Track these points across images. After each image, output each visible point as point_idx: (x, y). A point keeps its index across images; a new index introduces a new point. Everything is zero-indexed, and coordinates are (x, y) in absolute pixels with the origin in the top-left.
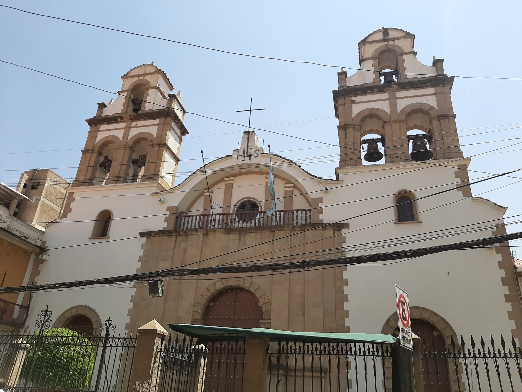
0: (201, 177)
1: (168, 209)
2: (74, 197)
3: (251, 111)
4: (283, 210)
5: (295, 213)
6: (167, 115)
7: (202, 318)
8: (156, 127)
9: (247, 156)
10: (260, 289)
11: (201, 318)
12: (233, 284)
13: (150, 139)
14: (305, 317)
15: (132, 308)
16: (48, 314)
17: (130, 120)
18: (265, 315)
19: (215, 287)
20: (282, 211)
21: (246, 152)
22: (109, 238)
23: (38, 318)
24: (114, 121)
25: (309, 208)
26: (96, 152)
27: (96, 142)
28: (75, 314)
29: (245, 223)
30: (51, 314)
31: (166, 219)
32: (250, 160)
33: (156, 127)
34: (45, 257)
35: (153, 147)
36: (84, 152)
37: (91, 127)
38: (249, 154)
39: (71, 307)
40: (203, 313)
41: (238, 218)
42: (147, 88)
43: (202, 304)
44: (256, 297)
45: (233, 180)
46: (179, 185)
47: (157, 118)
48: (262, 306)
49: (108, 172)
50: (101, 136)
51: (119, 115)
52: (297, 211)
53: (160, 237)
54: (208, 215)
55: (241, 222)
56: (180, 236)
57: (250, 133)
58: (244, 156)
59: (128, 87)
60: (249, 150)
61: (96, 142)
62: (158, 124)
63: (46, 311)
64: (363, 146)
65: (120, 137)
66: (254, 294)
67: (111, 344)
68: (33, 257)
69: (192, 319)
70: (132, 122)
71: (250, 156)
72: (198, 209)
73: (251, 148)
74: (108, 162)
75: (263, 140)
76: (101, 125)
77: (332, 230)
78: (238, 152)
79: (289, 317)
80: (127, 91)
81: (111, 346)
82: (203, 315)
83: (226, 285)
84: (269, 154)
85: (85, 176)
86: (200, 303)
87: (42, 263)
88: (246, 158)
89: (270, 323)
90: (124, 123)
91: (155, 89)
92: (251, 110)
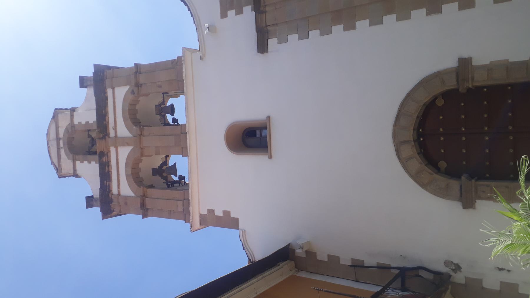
1: (224, 15)
2: (205, 212)
8: (117, 90)
13: (131, 97)
17: (105, 139)
22: (269, 118)
24: (107, 167)
31: (239, 12)
37: (114, 210)
42: (72, 127)
47: (105, 93)
53: (267, 9)
59: (70, 161)
68: (303, 275)
70: (109, 137)
76: (111, 192)
80: (74, 161)
87: (316, 253)
90: (110, 152)
91: (75, 113)
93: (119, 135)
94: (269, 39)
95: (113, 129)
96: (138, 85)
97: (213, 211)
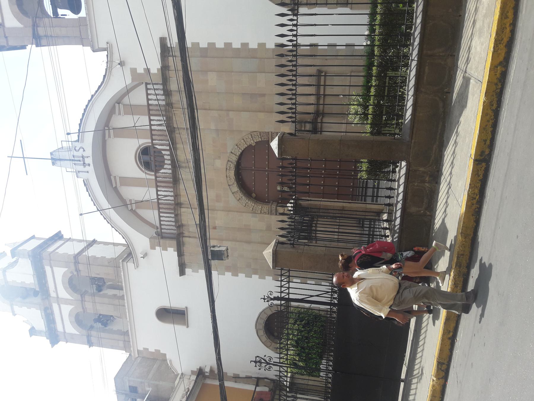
0: (112, 213)
1: (153, 247)
2: (142, 349)
3: (24, 157)
4: (148, 117)
5: (150, 102)
6: (39, 257)
7: (268, 204)
8: (55, 269)
9: (84, 161)
10: (238, 143)
11: (267, 205)
12: (233, 174)
13: (70, 275)
14: (265, 94)
15: (257, 276)
16: (259, 360)
18: (264, 138)
19: (237, 192)
20: (149, 118)
21: (79, 162)
23: (263, 370)
25: (144, 85)
26: (90, 333)
27: (78, 333)
28: (264, 331)
29: (166, 162)
30: (258, 357)
31: (165, 249)
32: (88, 157)
33: (55, 269)
34: (207, 370)
35: (80, 271)
36: (90, 344)
38: (81, 159)
39: (257, 336)
40: (263, 203)
41: (160, 170)
43: (253, 205)
44: (246, 148)
45: (115, 177)
46: (124, 238)
47: (43, 268)
48: (255, 141)
49: (113, 317)
50: (71, 329)
51: (43, 312)
52: (148, 100)
53: (185, 253)
54: (159, 204)
55: (165, 166)
56: (183, 233)
57: (54, 157)
58: (84, 164)
60: (76, 159)
61: (78, 333)
62: (51, 267)
63: (256, 362)
64: (62, 15)
65: (70, 307)
66: (244, 150)
67: (287, 294)
69: (268, 214)
70: (51, 297)
71: (83, 158)
72: (152, 215)
73: (74, 156)
74: (101, 318)
75: (62, 141)
77: (169, 57)
78: (79, 172)
79: (267, 112)
80: (12, 306)
81: (289, 294)
82: (265, 203)
83: (234, 181)
84: (79, 134)
85: (118, 340)
86: (253, 207)
87: (215, 371)
88: (86, 162)
89: (271, 132)
90: (52, 306)
92: (24, 158)
93: (60, 296)
94: (186, 268)
95: (54, 292)
96: (78, 270)
97: (148, 349)
